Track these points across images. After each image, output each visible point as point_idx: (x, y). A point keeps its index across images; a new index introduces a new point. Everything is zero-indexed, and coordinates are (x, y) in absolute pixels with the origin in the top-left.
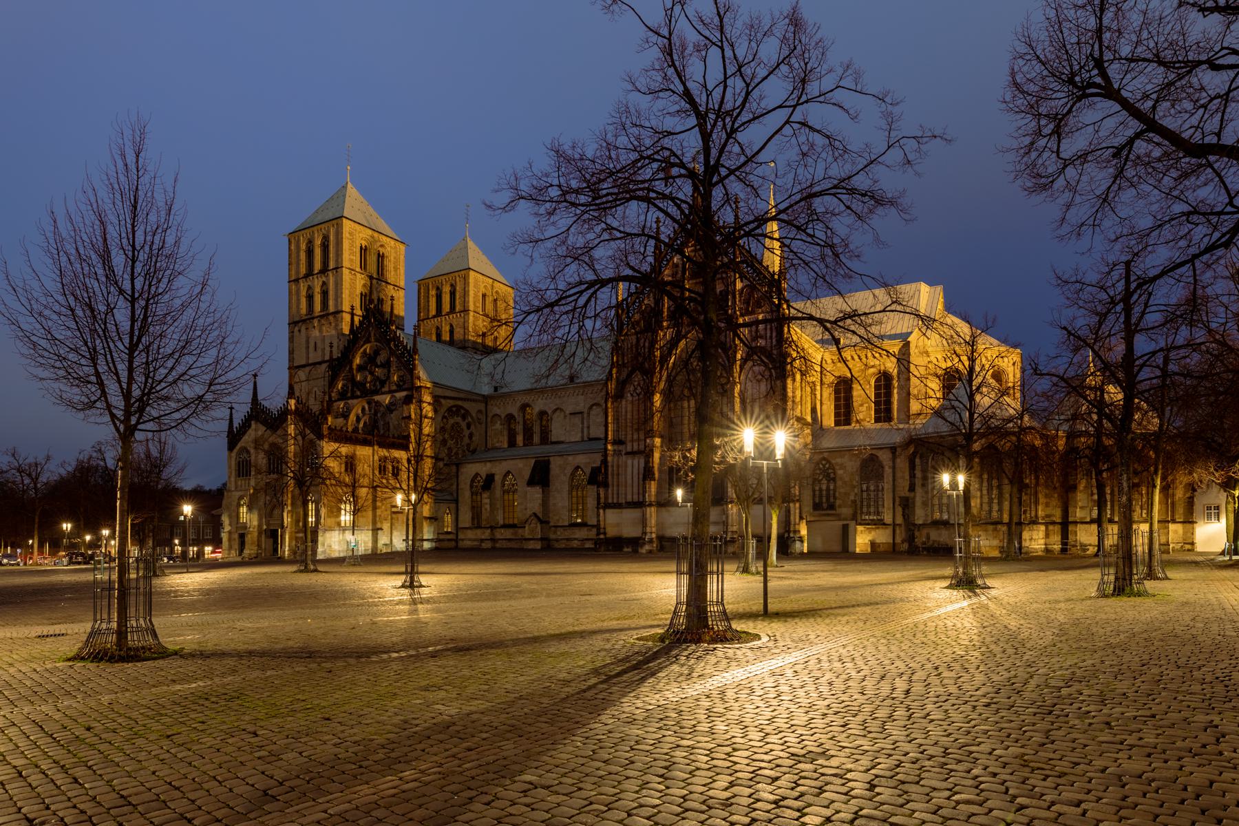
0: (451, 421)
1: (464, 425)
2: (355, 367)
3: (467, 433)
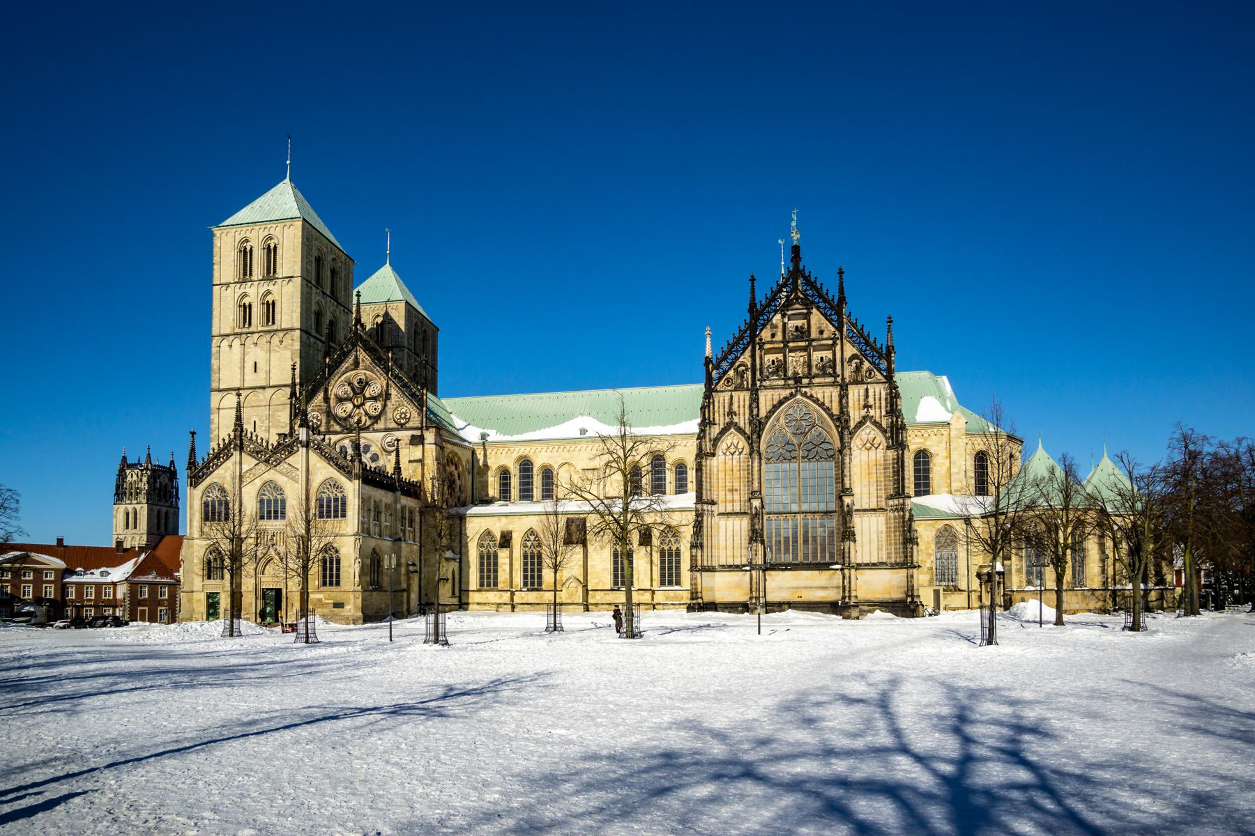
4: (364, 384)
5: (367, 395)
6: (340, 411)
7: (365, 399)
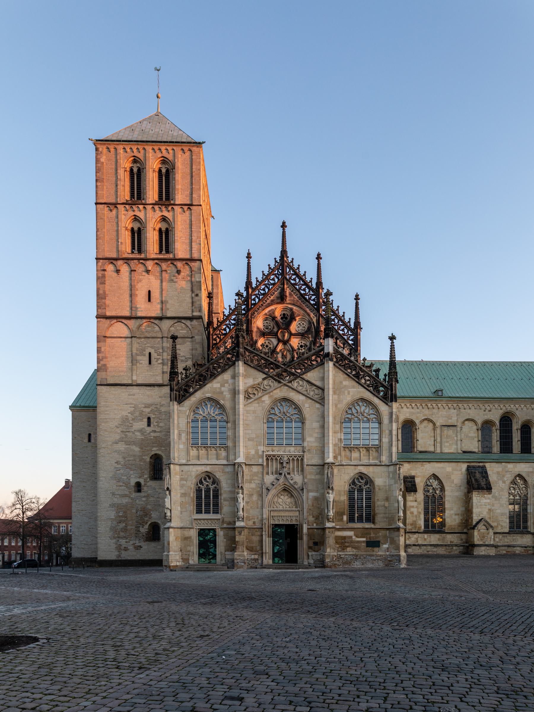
4: (288, 319)
5: (293, 332)
7: (291, 334)
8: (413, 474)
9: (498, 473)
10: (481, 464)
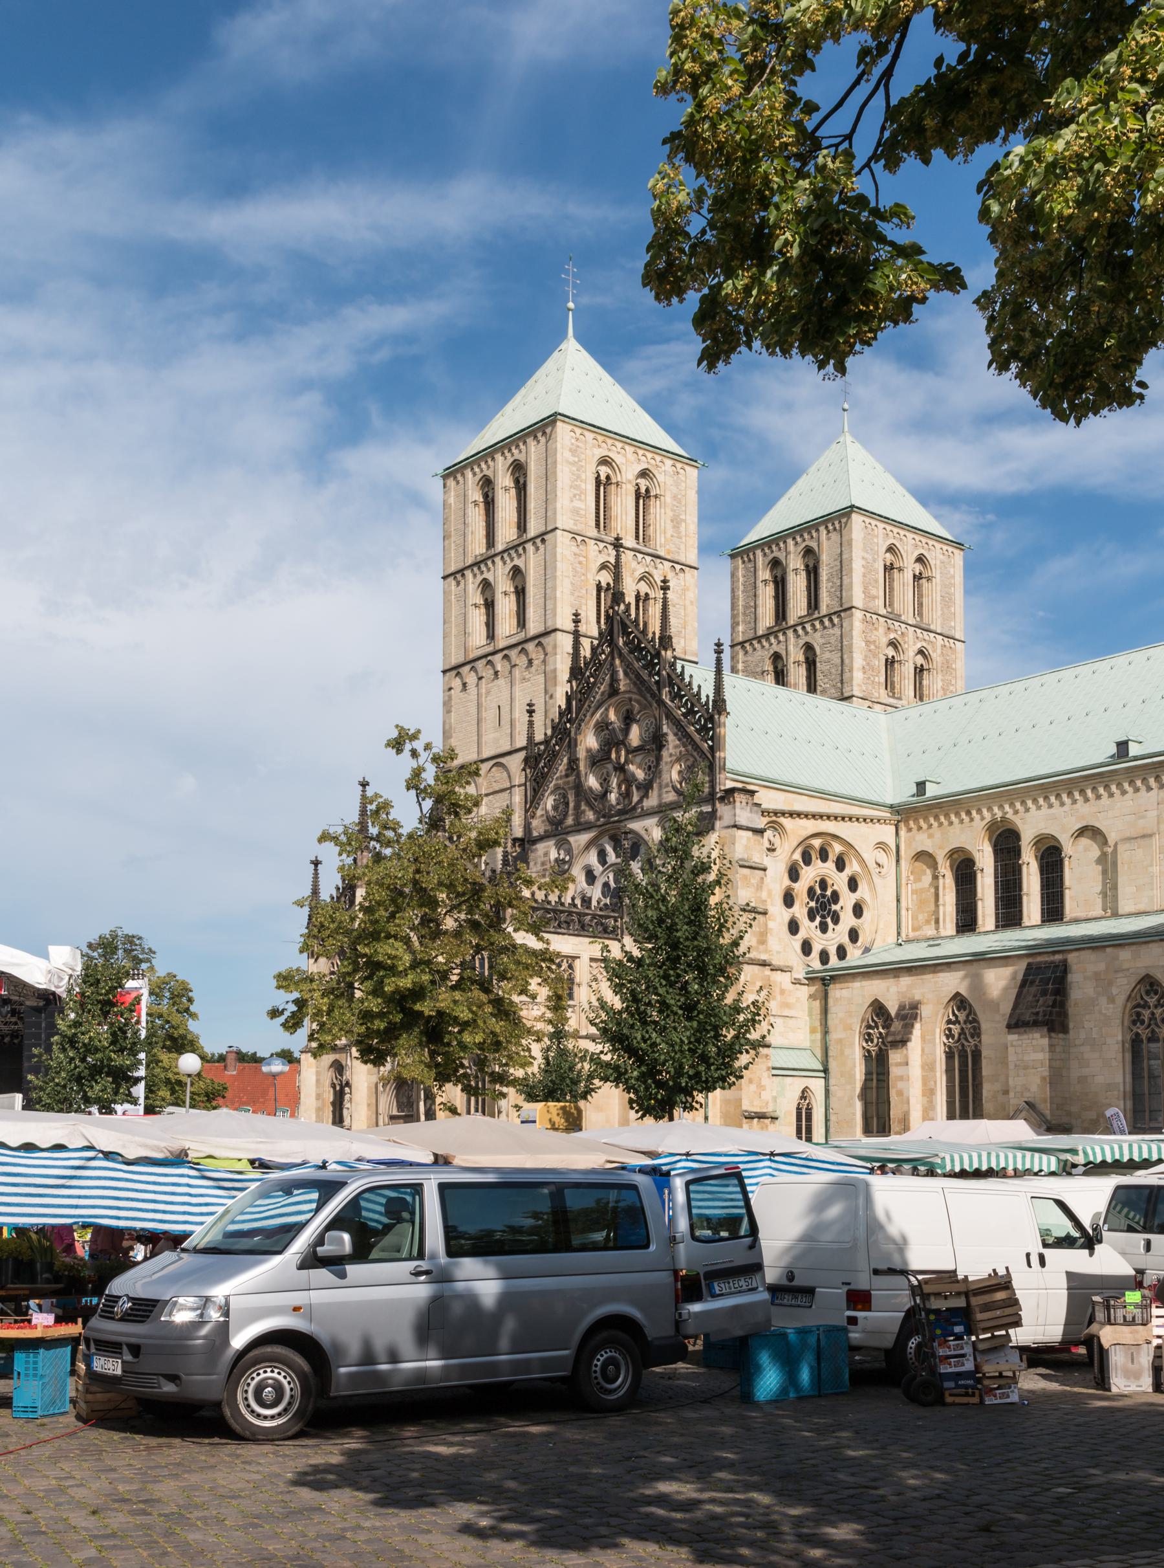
0: (809, 875)
1: (839, 882)
2: (581, 754)
3: (848, 899)
4: (628, 719)
6: (593, 782)
8: (917, 998)
9: (1097, 976)
10: (1058, 957)
